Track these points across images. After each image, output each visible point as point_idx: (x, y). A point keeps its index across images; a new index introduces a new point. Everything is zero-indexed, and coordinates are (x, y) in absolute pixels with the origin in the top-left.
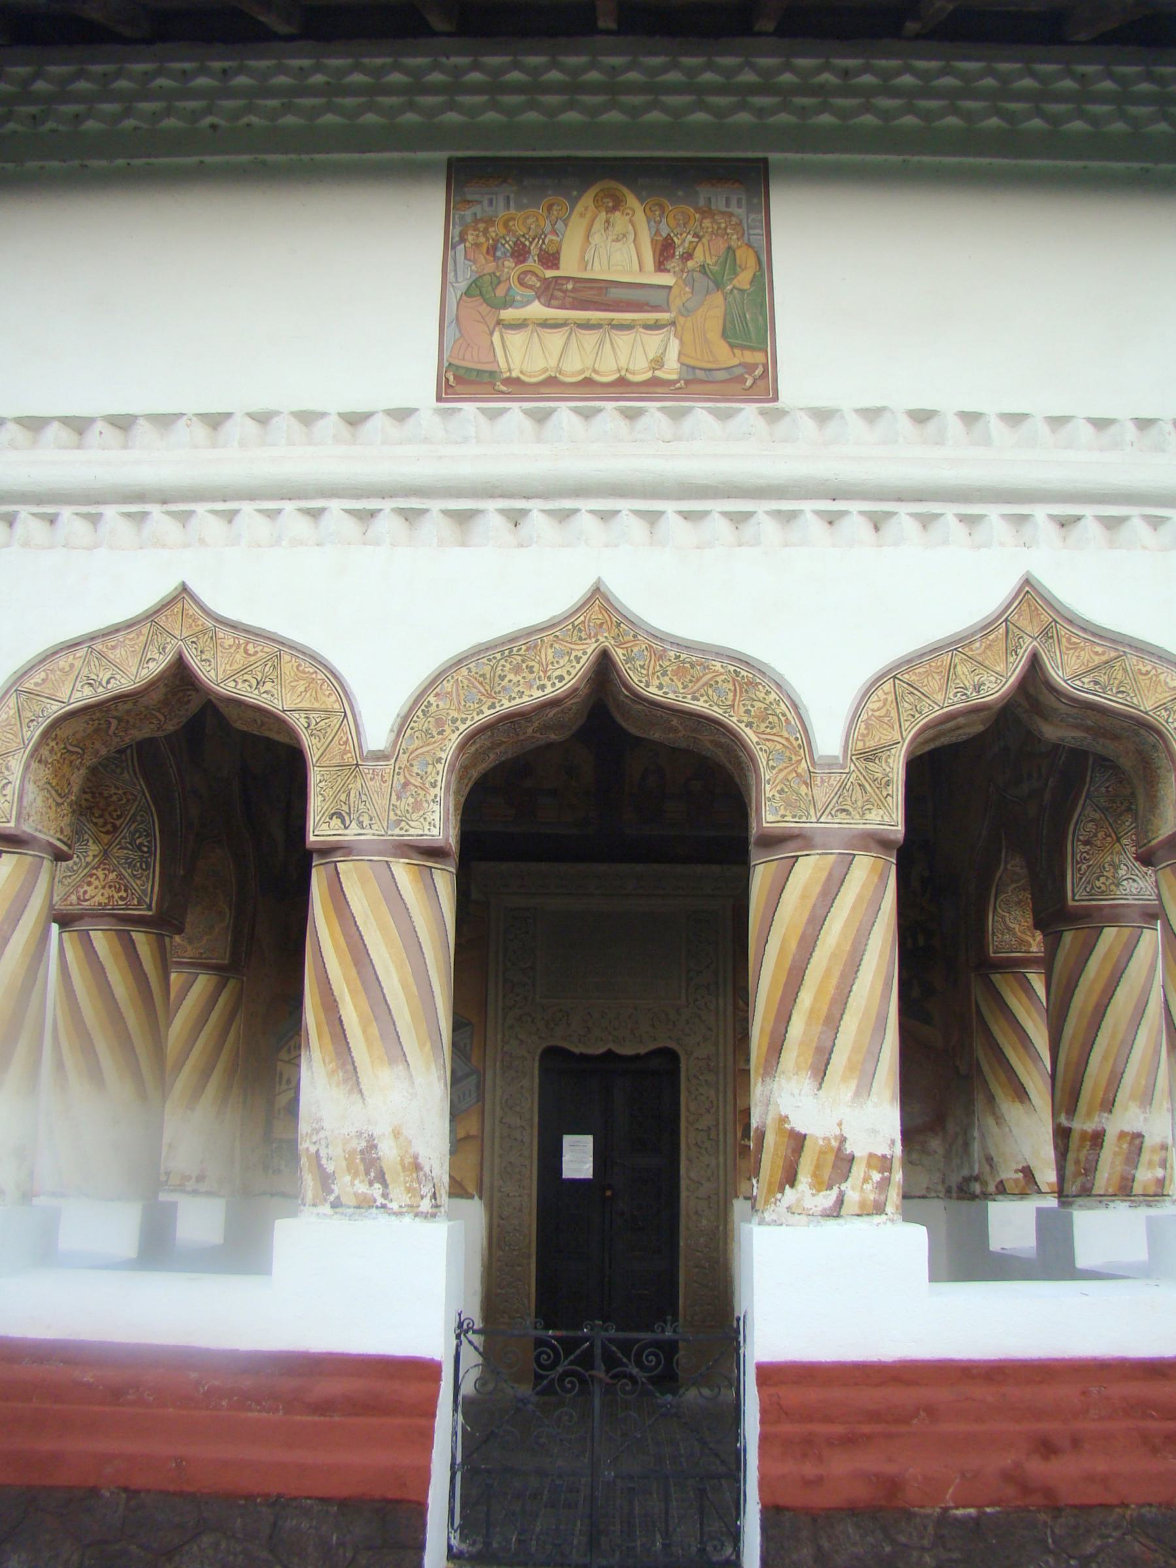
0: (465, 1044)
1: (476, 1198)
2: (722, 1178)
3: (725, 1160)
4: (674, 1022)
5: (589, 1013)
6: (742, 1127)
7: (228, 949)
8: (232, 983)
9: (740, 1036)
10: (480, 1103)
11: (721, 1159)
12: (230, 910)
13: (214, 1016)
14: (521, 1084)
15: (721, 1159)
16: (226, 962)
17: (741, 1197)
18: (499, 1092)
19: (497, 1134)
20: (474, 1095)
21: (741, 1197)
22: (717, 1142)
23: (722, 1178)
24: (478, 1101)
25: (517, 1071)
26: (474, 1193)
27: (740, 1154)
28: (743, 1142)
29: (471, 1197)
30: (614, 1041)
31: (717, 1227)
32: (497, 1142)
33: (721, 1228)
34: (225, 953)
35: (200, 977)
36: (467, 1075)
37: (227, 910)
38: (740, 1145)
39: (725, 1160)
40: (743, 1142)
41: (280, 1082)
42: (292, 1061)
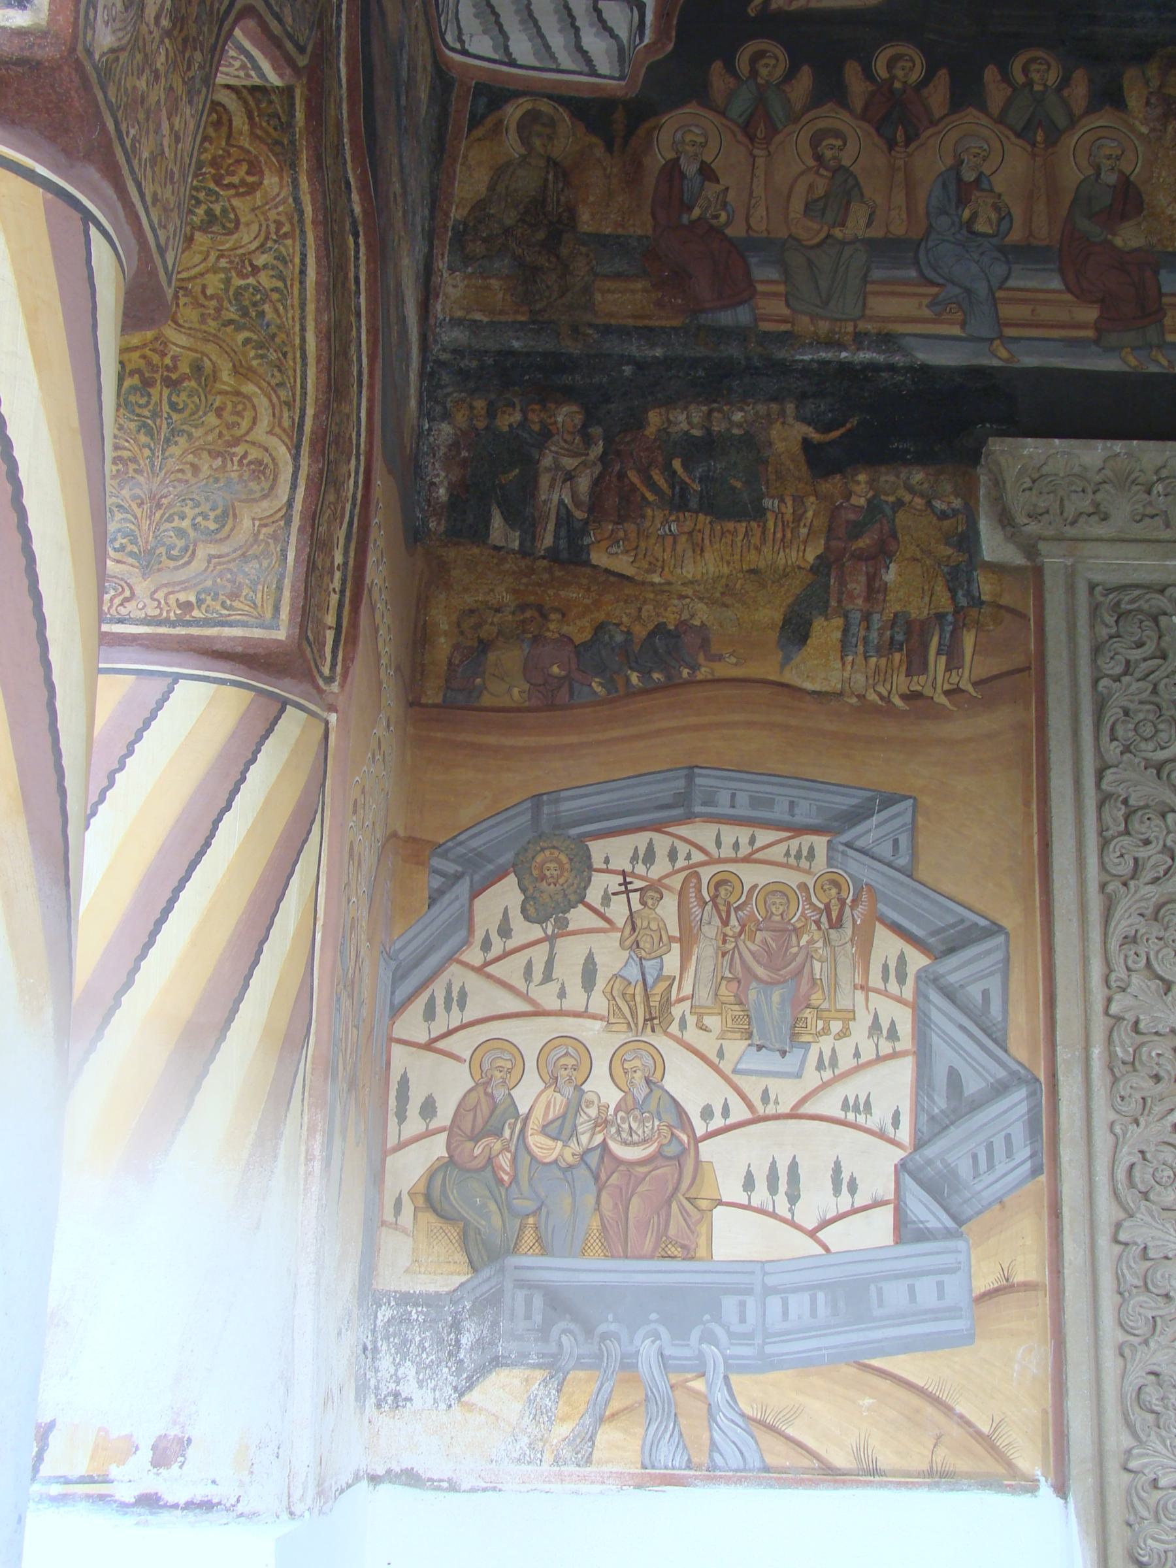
0: (986, 994)
1: (1046, 1490)
7: (287, 594)
8: (292, 723)
10: (1043, 1178)
12: (296, 458)
13: (261, 777)
16: (281, 635)
18: (1102, 1142)
24: (1036, 1171)
25: (1157, 1078)
26: (1038, 1472)
29: (1031, 1487)
32: (1108, 1301)
34: (277, 609)
35: (182, 686)
36: (1000, 1089)
37: (283, 453)
41: (401, 1116)
42: (441, 1045)
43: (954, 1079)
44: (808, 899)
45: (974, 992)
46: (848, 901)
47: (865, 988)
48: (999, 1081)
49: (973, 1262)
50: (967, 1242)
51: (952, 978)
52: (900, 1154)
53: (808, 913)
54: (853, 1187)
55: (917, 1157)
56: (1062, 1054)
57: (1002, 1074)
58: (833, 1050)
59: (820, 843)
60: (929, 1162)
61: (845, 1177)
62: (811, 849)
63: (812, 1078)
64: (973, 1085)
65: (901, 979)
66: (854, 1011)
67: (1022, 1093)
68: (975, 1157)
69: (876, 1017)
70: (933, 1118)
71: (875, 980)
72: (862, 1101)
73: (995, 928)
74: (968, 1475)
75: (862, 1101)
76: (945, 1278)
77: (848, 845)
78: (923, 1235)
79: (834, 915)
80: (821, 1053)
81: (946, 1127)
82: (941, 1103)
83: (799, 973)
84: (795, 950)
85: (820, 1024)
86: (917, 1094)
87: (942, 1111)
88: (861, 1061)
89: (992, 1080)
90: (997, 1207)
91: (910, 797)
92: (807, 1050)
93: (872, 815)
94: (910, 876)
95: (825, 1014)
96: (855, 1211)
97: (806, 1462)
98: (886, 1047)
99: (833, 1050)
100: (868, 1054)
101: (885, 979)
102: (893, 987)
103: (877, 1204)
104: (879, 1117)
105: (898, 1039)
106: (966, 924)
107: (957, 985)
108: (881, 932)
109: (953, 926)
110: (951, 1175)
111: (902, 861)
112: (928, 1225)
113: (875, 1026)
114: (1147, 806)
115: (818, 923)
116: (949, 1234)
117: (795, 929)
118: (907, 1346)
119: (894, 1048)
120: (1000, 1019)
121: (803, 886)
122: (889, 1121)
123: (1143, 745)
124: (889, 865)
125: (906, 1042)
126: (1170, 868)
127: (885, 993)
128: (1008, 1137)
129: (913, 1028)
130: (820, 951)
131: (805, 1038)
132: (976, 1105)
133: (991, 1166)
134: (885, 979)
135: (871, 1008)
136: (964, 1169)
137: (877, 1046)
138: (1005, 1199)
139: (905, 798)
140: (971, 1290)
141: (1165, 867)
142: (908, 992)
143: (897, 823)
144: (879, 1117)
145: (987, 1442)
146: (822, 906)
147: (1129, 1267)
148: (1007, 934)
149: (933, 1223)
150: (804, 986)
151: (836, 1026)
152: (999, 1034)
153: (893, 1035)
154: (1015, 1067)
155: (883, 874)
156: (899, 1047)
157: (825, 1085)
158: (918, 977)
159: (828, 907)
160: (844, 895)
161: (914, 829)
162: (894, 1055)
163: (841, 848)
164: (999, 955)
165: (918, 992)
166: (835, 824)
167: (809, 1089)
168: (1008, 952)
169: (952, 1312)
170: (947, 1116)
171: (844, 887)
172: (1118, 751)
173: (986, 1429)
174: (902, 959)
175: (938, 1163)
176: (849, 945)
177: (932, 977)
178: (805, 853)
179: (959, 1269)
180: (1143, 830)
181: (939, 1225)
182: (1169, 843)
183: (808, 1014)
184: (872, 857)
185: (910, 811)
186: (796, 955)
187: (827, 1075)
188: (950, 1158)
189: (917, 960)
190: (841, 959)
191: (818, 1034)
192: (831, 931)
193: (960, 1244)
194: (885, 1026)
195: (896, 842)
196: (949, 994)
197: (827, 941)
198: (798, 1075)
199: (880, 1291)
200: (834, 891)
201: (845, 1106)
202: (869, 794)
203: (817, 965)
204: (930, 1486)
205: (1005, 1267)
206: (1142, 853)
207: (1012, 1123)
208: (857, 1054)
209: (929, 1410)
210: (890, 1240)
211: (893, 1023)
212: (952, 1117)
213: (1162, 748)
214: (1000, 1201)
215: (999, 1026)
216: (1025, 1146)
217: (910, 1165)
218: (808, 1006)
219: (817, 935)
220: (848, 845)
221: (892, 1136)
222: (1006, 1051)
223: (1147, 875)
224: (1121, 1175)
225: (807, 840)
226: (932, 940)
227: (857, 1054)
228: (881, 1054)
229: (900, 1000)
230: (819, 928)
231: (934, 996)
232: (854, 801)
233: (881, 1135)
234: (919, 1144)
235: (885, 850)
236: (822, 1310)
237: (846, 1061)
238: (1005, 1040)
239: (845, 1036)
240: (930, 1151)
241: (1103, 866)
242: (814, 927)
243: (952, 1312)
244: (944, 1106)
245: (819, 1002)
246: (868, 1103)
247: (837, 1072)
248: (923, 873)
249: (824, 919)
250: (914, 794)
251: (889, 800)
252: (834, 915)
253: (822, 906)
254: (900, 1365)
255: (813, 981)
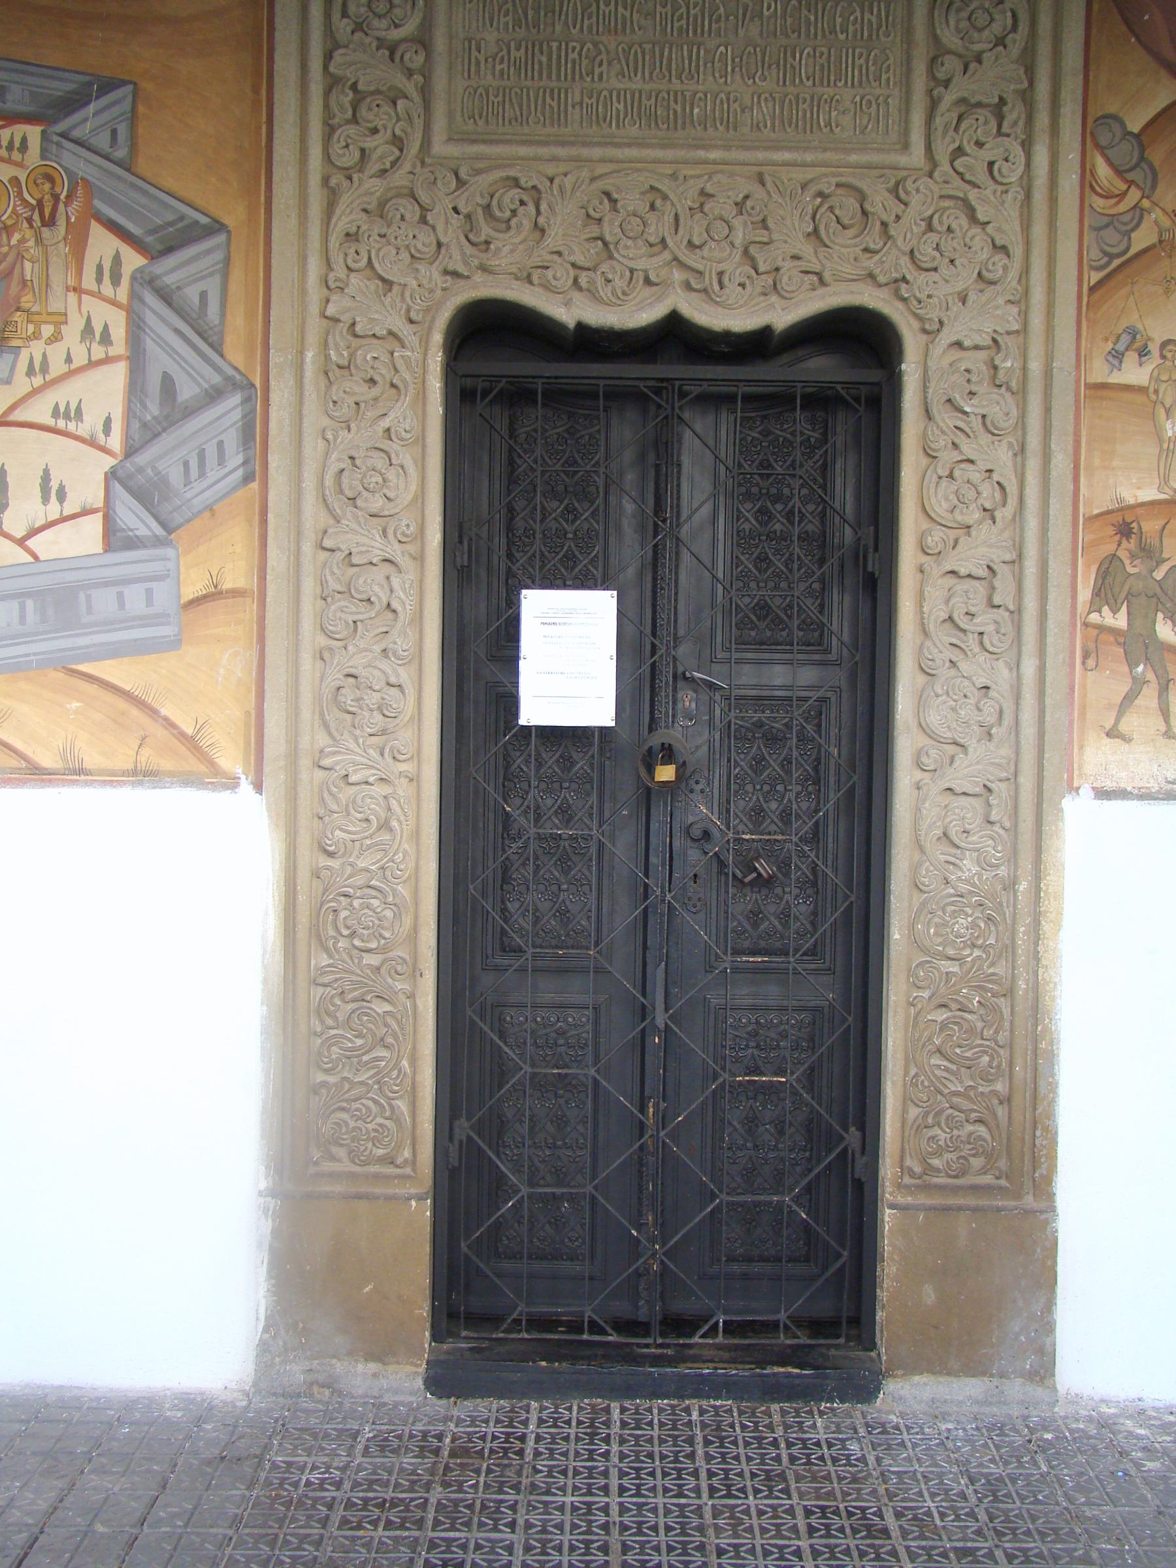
0: (203, 296)
1: (246, 787)
2: (1029, 731)
3: (1042, 669)
4: (884, 224)
5: (607, 194)
6: (1094, 568)
9: (1095, 277)
10: (255, 486)
11: (1029, 667)
14: (385, 423)
15: (1029, 667)
17: (1086, 792)
18: (313, 448)
19: (309, 587)
20: (235, 459)
21: (1086, 792)
22: (1017, 613)
23: (1029, 731)
24: (248, 479)
25: (372, 381)
26: (239, 770)
27: (1086, 656)
28: (1094, 617)
29: (232, 784)
30: (688, 286)
31: (1011, 885)
32: (309, 606)
33: (1023, 886)
36: (214, 395)
38: (1086, 625)
39: (1042, 669)
40: (1094, 617)
43: (168, 385)
44: (20, 193)
45: (192, 293)
46: (62, 197)
47: (78, 290)
48: (212, 387)
49: (182, 569)
50: (177, 549)
51: (170, 280)
52: (109, 462)
53: (20, 210)
54: (62, 496)
55: (128, 465)
56: (275, 358)
57: (217, 379)
58: (44, 355)
59: (34, 132)
60: (140, 470)
61: (54, 485)
62: (24, 140)
63: (22, 384)
64: (187, 391)
65: (116, 280)
66: (66, 315)
67: (236, 399)
68: (186, 464)
69: (89, 320)
70: (145, 425)
71: (89, 281)
72: (73, 408)
73: (217, 226)
74: (171, 774)
75: (73, 408)
76: (154, 585)
77: (64, 135)
78: (132, 543)
79: (47, 211)
80: (32, 359)
81: (159, 434)
82: (154, 409)
83: (9, 273)
84: (5, 249)
85: (31, 328)
86: (130, 401)
87: (154, 418)
88: (73, 367)
89: (206, 386)
90: (207, 514)
91: (130, 82)
92: (17, 355)
93: (88, 103)
94: (128, 170)
95: (36, 318)
96: (64, 519)
97: (14, 763)
98: (98, 352)
99: (44, 355)
100: (80, 360)
101: (99, 280)
102: (107, 289)
103: (86, 512)
104: (90, 424)
105: (111, 343)
106: (185, 222)
107: (174, 287)
108: (97, 231)
109: (171, 224)
110: (162, 482)
111: (121, 153)
112: (138, 533)
113: (88, 330)
114: (378, 92)
115: (29, 220)
116: (158, 542)
117: (6, 228)
118: (115, 652)
119: (107, 353)
120: (217, 322)
121: (15, 181)
122: (100, 427)
123: (376, 23)
124: (107, 157)
125: (119, 347)
126: (398, 159)
127: (99, 295)
128: (221, 444)
129: (127, 332)
130: (32, 251)
131: (15, 343)
132: (190, 412)
133: (202, 474)
134: (99, 280)
135: (84, 311)
136: (175, 476)
137: (89, 350)
138: (215, 507)
139: (124, 83)
140: (179, 597)
141: (392, 158)
142: (123, 295)
143: (116, 111)
144: (90, 424)
145: (191, 743)
146: (34, 202)
147: (333, 573)
148: (229, 232)
149: (142, 531)
150: (14, 288)
151: (47, 330)
152: (215, 338)
153: (106, 339)
154: (230, 372)
155: (100, 167)
156: (113, 351)
157: (35, 392)
158: (133, 278)
159: (40, 203)
160: (58, 190)
161: (133, 119)
162: (107, 360)
163: (56, 138)
164: (219, 256)
165: (133, 295)
166: (51, 112)
167: (19, 396)
168: (229, 252)
169: (158, 619)
170: (159, 423)
171: (58, 181)
172: (349, 29)
173: (189, 731)
174: (117, 260)
175: (149, 471)
176: (62, 245)
177: (147, 278)
178: (17, 144)
179: (168, 576)
180: (371, 117)
181: (149, 533)
182: (398, 132)
183: (18, 316)
184: (89, 149)
185: (130, 99)
186: (6, 255)
187: (38, 381)
188: (160, 466)
189: (133, 261)
190: (53, 259)
191: (28, 339)
192: (43, 229)
193: (170, 552)
194: (98, 330)
195: (114, 133)
196: (166, 296)
197: (39, 240)
198: (8, 382)
199: (89, 598)
200: (47, 186)
201: (56, 413)
202: (87, 78)
203: (28, 266)
204: (134, 784)
205: (214, 574)
206: (369, 143)
207: (225, 430)
208: (69, 360)
209: (135, 712)
210: (98, 548)
211: (106, 327)
212: (165, 424)
213: (397, 26)
214: (210, 508)
215: (216, 329)
216: (238, 453)
217: (120, 473)
218: (18, 309)
219: (29, 233)
220: (64, 135)
221: (103, 443)
222: (222, 356)
223: (373, 167)
224: (329, 481)
225: (20, 130)
226: (149, 239)
227: (69, 360)
228: (93, 359)
229: (114, 303)
230: (31, 226)
231: (150, 298)
232: (71, 87)
233: (91, 442)
234: (130, 451)
235: (102, 141)
236: (31, 616)
237: (57, 367)
238: (221, 345)
239: (57, 340)
240: (142, 459)
241: (327, 158)
242: (25, 225)
243: (158, 619)
244: (156, 412)
245: (29, 305)
246: (79, 410)
247: (48, 378)
248: (142, 166)
249: (36, 217)
250: (135, 79)
251: (108, 86)
252: (47, 211)
253: (34, 202)
254: (107, 670)
255: (24, 283)
